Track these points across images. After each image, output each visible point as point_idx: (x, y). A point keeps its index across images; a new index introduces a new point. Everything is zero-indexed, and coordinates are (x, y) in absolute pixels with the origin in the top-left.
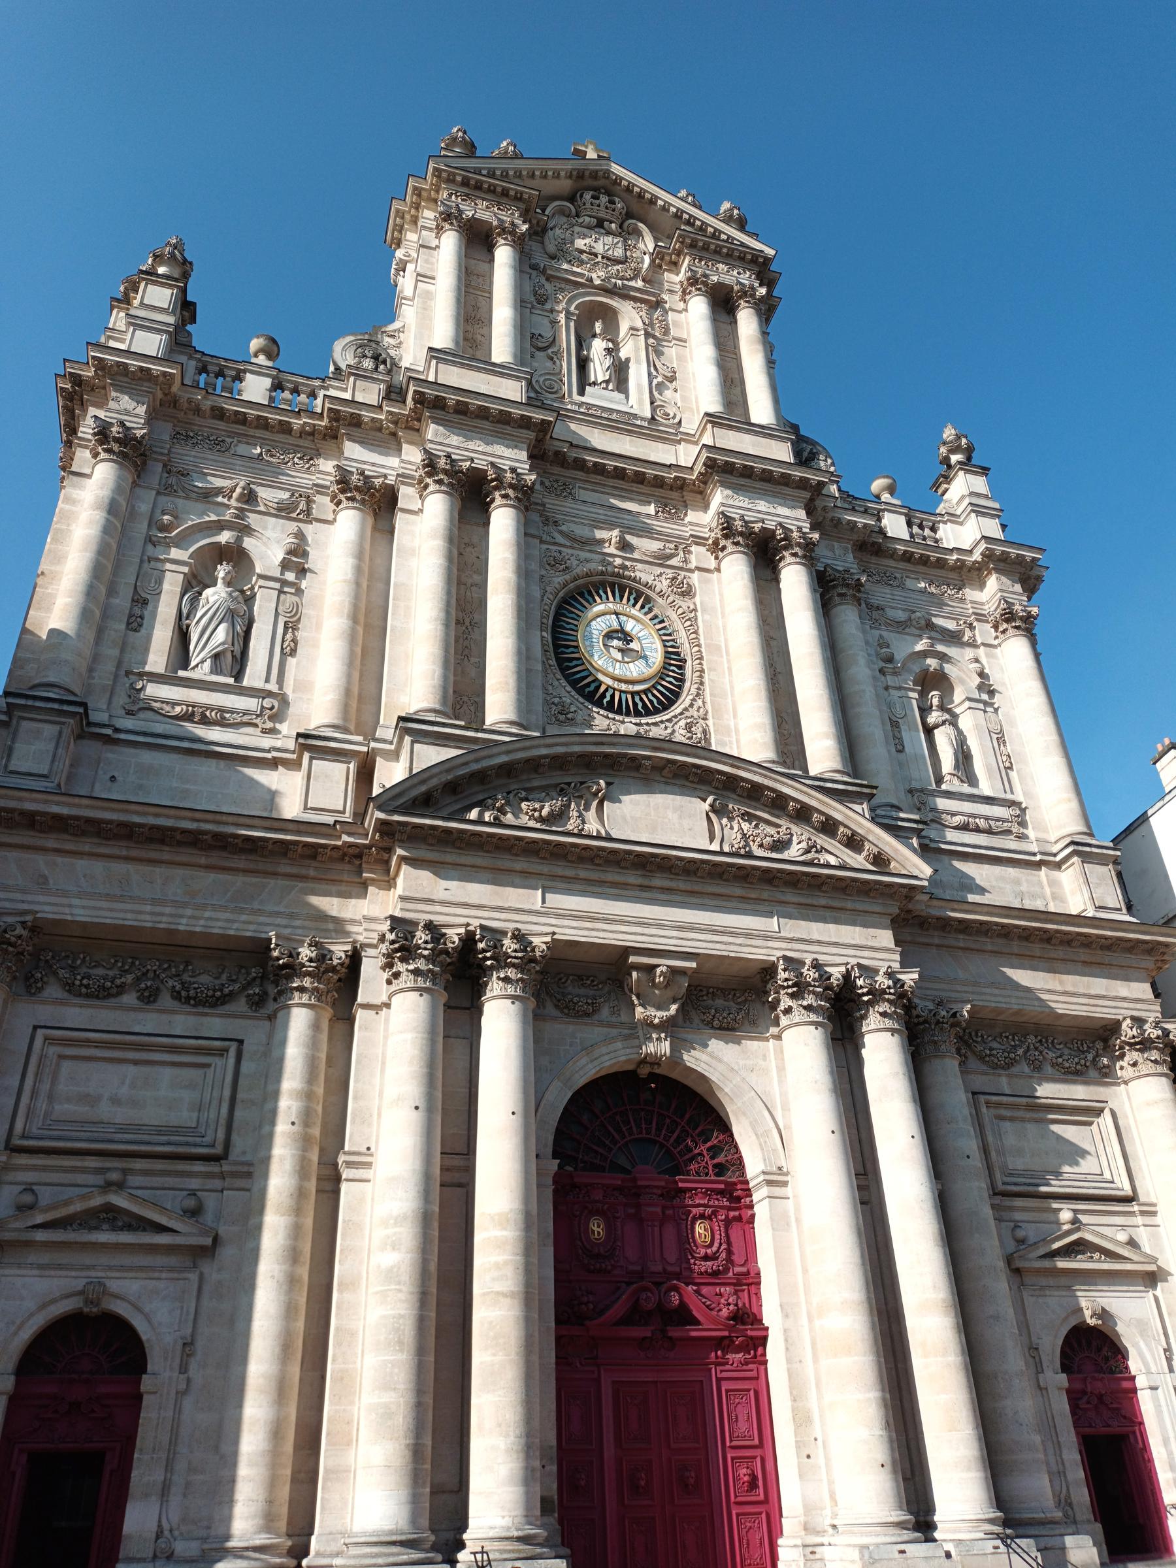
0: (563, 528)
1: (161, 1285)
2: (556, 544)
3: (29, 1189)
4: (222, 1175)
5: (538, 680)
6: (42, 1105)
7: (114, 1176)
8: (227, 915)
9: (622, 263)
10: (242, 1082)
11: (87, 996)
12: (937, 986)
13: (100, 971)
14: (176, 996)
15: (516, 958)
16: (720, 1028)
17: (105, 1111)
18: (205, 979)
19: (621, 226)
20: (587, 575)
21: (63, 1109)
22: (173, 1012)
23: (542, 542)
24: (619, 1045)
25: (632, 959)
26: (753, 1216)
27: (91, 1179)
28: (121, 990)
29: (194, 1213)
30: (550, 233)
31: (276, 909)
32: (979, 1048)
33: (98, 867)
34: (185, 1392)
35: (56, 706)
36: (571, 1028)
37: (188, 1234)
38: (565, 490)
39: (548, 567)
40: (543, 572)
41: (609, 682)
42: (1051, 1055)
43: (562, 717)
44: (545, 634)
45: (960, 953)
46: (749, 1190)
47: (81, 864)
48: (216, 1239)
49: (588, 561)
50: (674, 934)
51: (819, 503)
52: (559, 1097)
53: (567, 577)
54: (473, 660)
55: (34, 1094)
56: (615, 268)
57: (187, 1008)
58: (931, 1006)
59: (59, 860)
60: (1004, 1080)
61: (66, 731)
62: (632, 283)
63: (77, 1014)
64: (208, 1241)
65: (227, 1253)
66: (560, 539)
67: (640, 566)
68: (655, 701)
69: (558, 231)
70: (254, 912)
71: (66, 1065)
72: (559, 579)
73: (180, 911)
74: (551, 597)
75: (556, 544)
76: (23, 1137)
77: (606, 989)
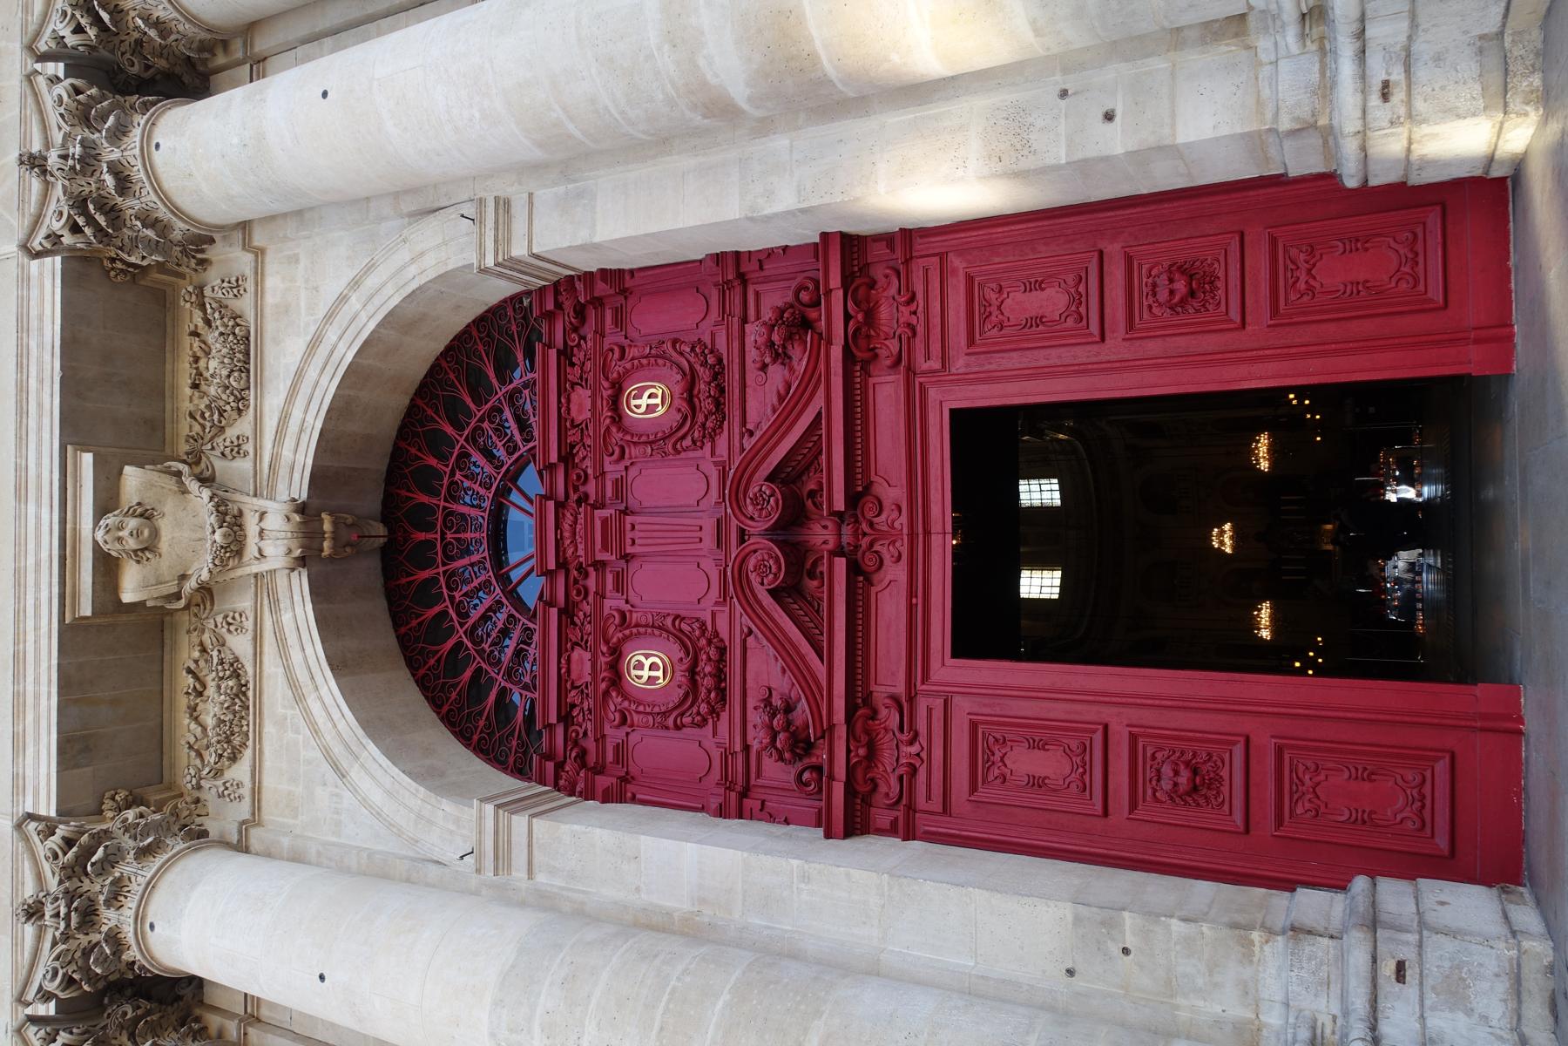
15: (68, 918)
24: (287, 617)
25: (86, 610)
26: (604, 273)
36: (269, 729)
46: (556, 285)
50: (31, 508)
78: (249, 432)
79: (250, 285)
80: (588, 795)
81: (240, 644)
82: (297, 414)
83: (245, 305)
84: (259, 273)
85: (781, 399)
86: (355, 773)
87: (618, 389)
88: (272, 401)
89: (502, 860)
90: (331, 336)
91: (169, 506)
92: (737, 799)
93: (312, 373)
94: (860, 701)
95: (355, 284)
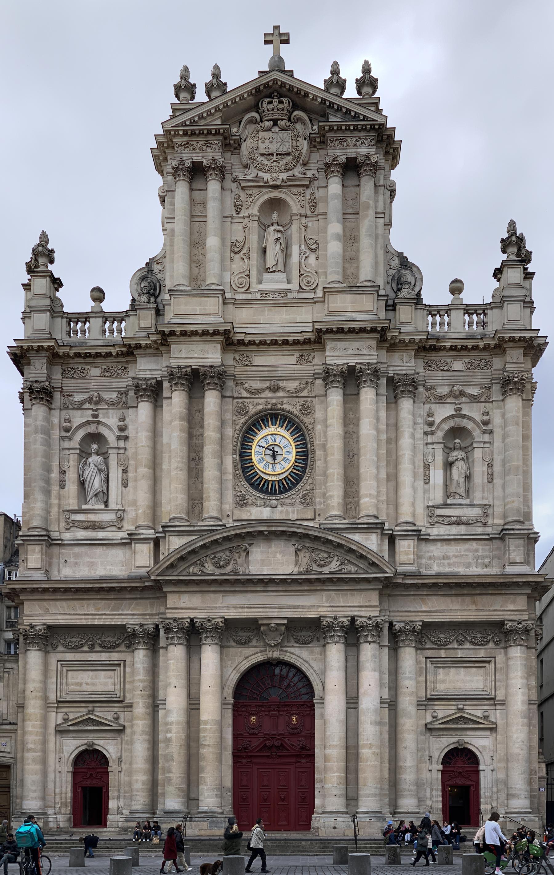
0: (246, 385)
1: (110, 741)
2: (241, 398)
3: (66, 714)
4: (124, 707)
5: (229, 485)
6: (64, 687)
7: (90, 709)
8: (110, 617)
9: (288, 154)
10: (127, 675)
11: (72, 649)
12: (410, 614)
13: (74, 639)
14: (101, 646)
16: (303, 644)
17: (84, 687)
18: (109, 639)
19: (289, 120)
20: (258, 413)
21: (71, 688)
22: (101, 652)
23: (234, 398)
24: (259, 654)
27: (84, 710)
28: (82, 646)
29: (117, 718)
30: (244, 145)
31: (128, 612)
32: (432, 638)
33: (64, 603)
34: (120, 772)
35: (37, 538)
36: (240, 649)
37: (115, 727)
38: (246, 361)
39: (237, 414)
40: (235, 418)
41: (266, 477)
42: (469, 638)
43: (241, 503)
44: (235, 456)
45: (425, 597)
47: (58, 603)
48: (124, 727)
49: (258, 404)
51: (389, 335)
52: (233, 677)
53: (247, 418)
54: (200, 479)
55: (61, 684)
56: (284, 161)
57: (105, 650)
58: (403, 624)
59: (51, 602)
60: (443, 651)
61: (44, 547)
62: (297, 172)
63: (69, 656)
64: (122, 728)
65: (128, 731)
66: (245, 394)
67: (285, 400)
68: (289, 483)
69: (249, 141)
70: (119, 615)
71: (70, 673)
72: (242, 421)
73: (94, 617)
74: (238, 432)
75: (241, 398)
76: (61, 698)
77: (255, 632)
78: (291, 644)
79: (318, 644)
80: (234, 711)
81: (254, 643)
82: (294, 657)
83: (314, 643)
84: (318, 646)
85: (293, 745)
86: (235, 672)
87: (297, 714)
88: (296, 651)
89: (225, 704)
90: (307, 665)
91: (278, 633)
92: (235, 737)
93: (301, 660)
94: (251, 756)
95: (315, 671)
